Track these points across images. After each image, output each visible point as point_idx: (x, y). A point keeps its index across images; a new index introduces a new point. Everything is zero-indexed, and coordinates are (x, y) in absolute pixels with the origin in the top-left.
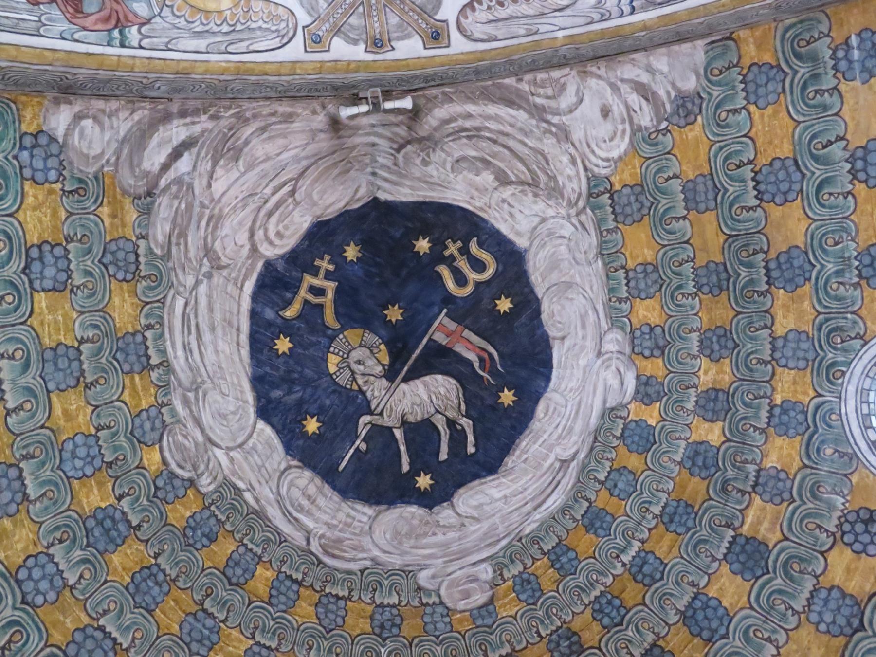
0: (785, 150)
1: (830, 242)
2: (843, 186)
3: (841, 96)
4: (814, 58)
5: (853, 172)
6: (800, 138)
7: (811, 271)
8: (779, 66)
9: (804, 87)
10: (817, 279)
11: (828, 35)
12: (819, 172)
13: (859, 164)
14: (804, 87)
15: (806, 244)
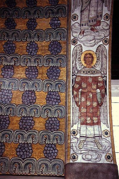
0: (38, 4)
1: (16, 12)
2: (28, 17)
3: (47, 18)
4: (57, 13)
5: (31, 19)
6: (41, 8)
7: (10, 7)
8: (58, 5)
9: (52, 10)
10: (9, 9)
11: (61, 17)
12: (32, 12)
13: (33, 20)
14: (52, 10)
15: (17, 7)
